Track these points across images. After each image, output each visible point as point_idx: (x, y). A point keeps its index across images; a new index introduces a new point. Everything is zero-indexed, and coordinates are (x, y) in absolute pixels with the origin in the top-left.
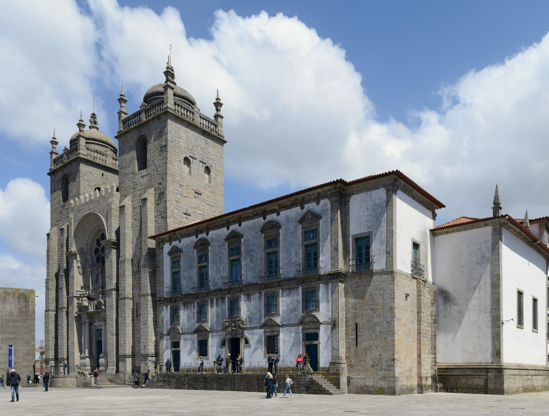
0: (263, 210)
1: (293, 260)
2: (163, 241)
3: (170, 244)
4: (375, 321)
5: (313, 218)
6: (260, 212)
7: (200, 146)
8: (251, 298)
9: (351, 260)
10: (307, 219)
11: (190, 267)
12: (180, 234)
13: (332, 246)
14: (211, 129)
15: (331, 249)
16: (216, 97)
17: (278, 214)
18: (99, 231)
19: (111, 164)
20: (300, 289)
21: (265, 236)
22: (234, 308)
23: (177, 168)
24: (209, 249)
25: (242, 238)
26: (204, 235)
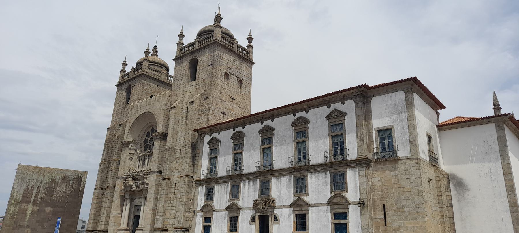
0: (294, 108)
1: (321, 148)
2: (205, 134)
3: (210, 136)
4: (403, 203)
5: (339, 114)
6: (291, 110)
7: (236, 66)
8: (281, 180)
9: (375, 149)
10: (333, 115)
11: (226, 154)
12: (220, 128)
13: (357, 137)
14: (244, 55)
15: (357, 139)
16: (249, 34)
17: (307, 112)
18: (150, 126)
19: (164, 79)
20: (328, 173)
21: (295, 129)
22: (265, 189)
23: (219, 80)
24: (244, 139)
25: (274, 131)
26: (240, 129)
